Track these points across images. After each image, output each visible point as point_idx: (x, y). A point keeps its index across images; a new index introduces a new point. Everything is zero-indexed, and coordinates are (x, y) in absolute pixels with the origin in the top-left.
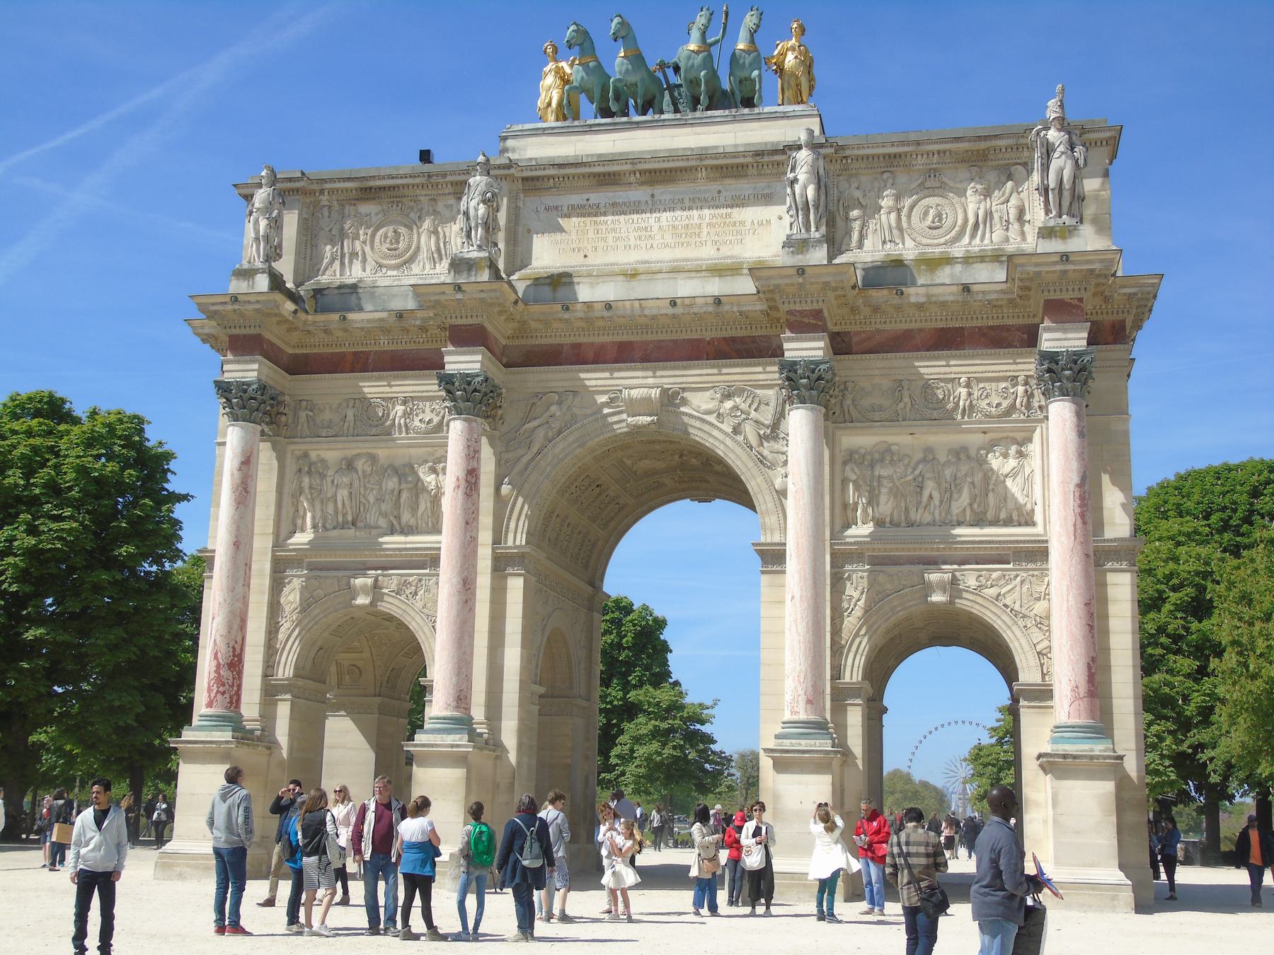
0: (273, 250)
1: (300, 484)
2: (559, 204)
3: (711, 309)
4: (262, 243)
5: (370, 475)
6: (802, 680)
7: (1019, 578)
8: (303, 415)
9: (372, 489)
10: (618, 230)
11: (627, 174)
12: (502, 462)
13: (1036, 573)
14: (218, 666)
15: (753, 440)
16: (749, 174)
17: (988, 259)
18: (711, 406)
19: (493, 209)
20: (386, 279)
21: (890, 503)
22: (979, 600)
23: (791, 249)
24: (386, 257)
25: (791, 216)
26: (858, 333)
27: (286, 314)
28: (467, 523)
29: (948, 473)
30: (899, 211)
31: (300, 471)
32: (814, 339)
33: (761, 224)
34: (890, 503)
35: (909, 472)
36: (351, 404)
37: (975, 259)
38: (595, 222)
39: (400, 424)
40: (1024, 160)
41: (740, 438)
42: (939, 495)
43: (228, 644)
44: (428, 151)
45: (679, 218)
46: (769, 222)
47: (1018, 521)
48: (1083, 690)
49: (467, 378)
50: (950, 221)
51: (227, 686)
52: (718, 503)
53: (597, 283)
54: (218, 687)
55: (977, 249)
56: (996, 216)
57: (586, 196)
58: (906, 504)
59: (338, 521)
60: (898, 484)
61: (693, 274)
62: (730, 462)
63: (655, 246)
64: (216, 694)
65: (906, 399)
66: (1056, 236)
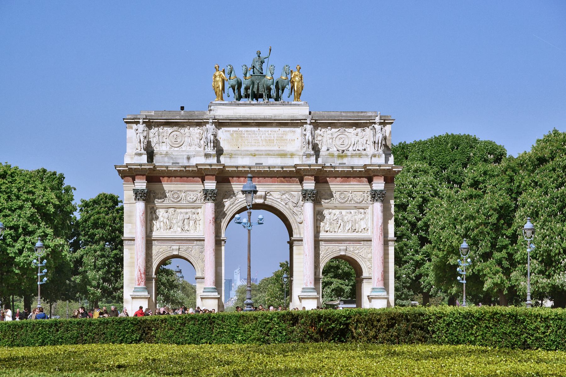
3: (280, 169)
7: (364, 248)
8: (152, 195)
14: (141, 274)
17: (357, 156)
18: (279, 197)
20: (175, 151)
22: (354, 254)
26: (321, 177)
31: (151, 212)
33: (292, 140)
41: (287, 206)
44: (183, 107)
46: (294, 140)
48: (380, 278)
49: (212, 191)
50: (347, 143)
57: (238, 128)
61: (273, 156)
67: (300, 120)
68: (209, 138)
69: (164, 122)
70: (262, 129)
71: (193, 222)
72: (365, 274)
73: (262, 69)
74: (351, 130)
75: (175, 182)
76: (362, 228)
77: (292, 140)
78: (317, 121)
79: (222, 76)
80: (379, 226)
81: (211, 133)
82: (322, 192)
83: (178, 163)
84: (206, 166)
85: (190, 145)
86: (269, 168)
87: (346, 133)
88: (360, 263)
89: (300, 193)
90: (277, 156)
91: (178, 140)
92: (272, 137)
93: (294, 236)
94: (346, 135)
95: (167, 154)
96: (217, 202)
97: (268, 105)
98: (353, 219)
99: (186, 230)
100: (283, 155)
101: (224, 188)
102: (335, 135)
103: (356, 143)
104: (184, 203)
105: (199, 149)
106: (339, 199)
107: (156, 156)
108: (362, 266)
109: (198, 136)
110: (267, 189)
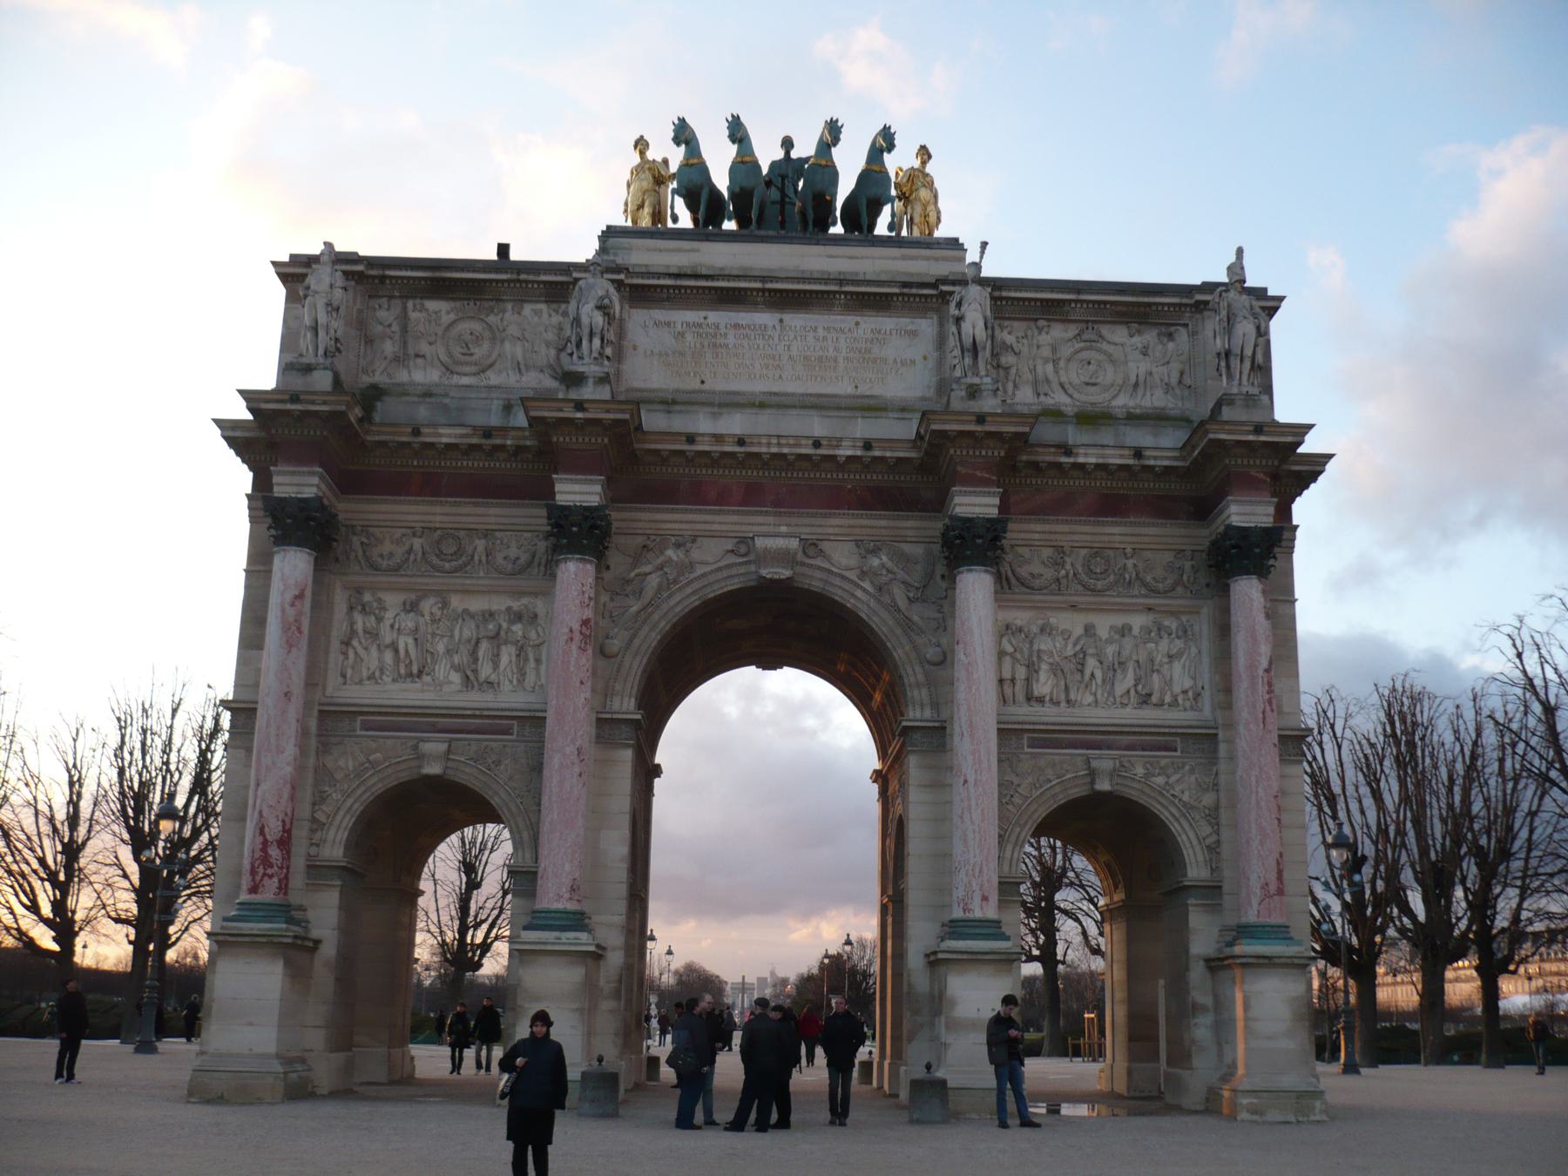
0: (333, 342)
1: (352, 627)
3: (859, 453)
4: (321, 333)
5: (439, 620)
6: (977, 874)
7: (1187, 767)
8: (356, 540)
9: (442, 636)
11: (755, 293)
12: (607, 615)
13: (1202, 761)
14: (265, 843)
15: (902, 603)
17: (1152, 422)
18: (853, 562)
19: (609, 318)
21: (1050, 682)
22: (1147, 790)
24: (457, 363)
27: (352, 419)
28: (582, 683)
29: (1110, 650)
30: (1055, 362)
31: (351, 609)
32: (989, 494)
33: (903, 363)
34: (1050, 682)
35: (1070, 646)
36: (419, 534)
39: (480, 561)
41: (886, 599)
42: (1101, 675)
43: (277, 816)
45: (812, 349)
47: (1183, 705)
48: (1273, 888)
51: (275, 868)
52: (788, 672)
53: (721, 414)
54: (265, 869)
56: (1156, 377)
57: (703, 314)
58: (1065, 678)
59: (400, 675)
60: (1057, 659)
62: (874, 626)
63: (784, 377)
64: (263, 877)
65: (1068, 567)
67: (934, 285)
68: (585, 320)
70: (796, 320)
71: (512, 650)
72: (1196, 871)
74: (1118, 334)
75: (451, 496)
76: (1177, 689)
77: (903, 363)
78: (997, 294)
80: (1261, 672)
81: (591, 305)
82: (1020, 550)
84: (561, 410)
85: (519, 369)
86: (817, 444)
87: (1105, 346)
88: (1175, 827)
89: (937, 548)
90: (848, 414)
91: (472, 351)
92: (831, 350)
93: (911, 715)
94: (1105, 353)
95: (428, 394)
96: (607, 576)
98: (1142, 657)
99: (483, 676)
100: (872, 407)
101: (641, 525)
102: (1066, 351)
103: (1141, 379)
104: (482, 574)
106: (1086, 579)
107: (387, 399)
108: (1182, 839)
109: (550, 336)
110: (807, 530)
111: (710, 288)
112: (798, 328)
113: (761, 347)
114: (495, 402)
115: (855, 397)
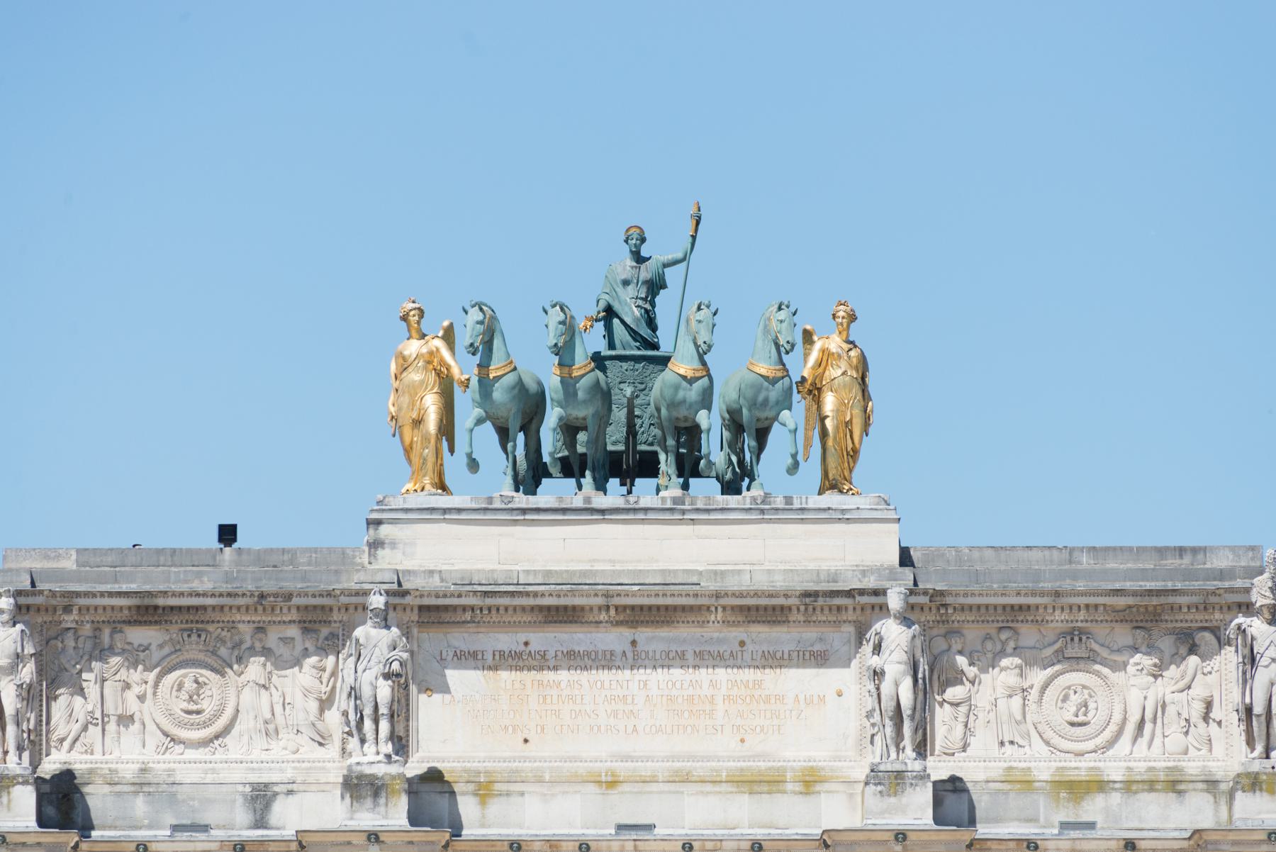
2: (480, 649)
10: (579, 698)
16: (791, 619)
17: (1159, 787)
23: (879, 788)
25: (873, 725)
33: (809, 702)
37: (1140, 786)
38: (540, 683)
40: (1215, 624)
45: (678, 685)
46: (822, 699)
53: (553, 795)
55: (1142, 766)
56: (1171, 710)
57: (522, 637)
61: (709, 787)
66: (1261, 790)
68: (366, 692)
69: (130, 608)
73: (651, 323)
77: (809, 702)
79: (442, 362)
81: (377, 669)
83: (205, 828)
92: (705, 685)
97: (683, 512)
103: (1148, 715)
105: (320, 753)
111: (532, 608)
112: (658, 656)
113: (607, 684)
114: (240, 788)
115: (744, 759)
